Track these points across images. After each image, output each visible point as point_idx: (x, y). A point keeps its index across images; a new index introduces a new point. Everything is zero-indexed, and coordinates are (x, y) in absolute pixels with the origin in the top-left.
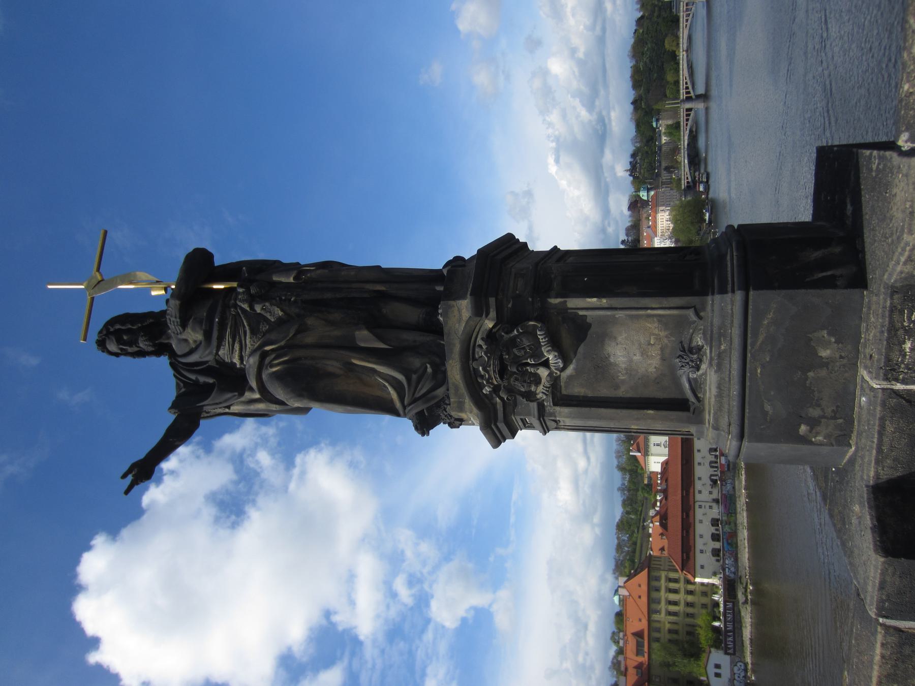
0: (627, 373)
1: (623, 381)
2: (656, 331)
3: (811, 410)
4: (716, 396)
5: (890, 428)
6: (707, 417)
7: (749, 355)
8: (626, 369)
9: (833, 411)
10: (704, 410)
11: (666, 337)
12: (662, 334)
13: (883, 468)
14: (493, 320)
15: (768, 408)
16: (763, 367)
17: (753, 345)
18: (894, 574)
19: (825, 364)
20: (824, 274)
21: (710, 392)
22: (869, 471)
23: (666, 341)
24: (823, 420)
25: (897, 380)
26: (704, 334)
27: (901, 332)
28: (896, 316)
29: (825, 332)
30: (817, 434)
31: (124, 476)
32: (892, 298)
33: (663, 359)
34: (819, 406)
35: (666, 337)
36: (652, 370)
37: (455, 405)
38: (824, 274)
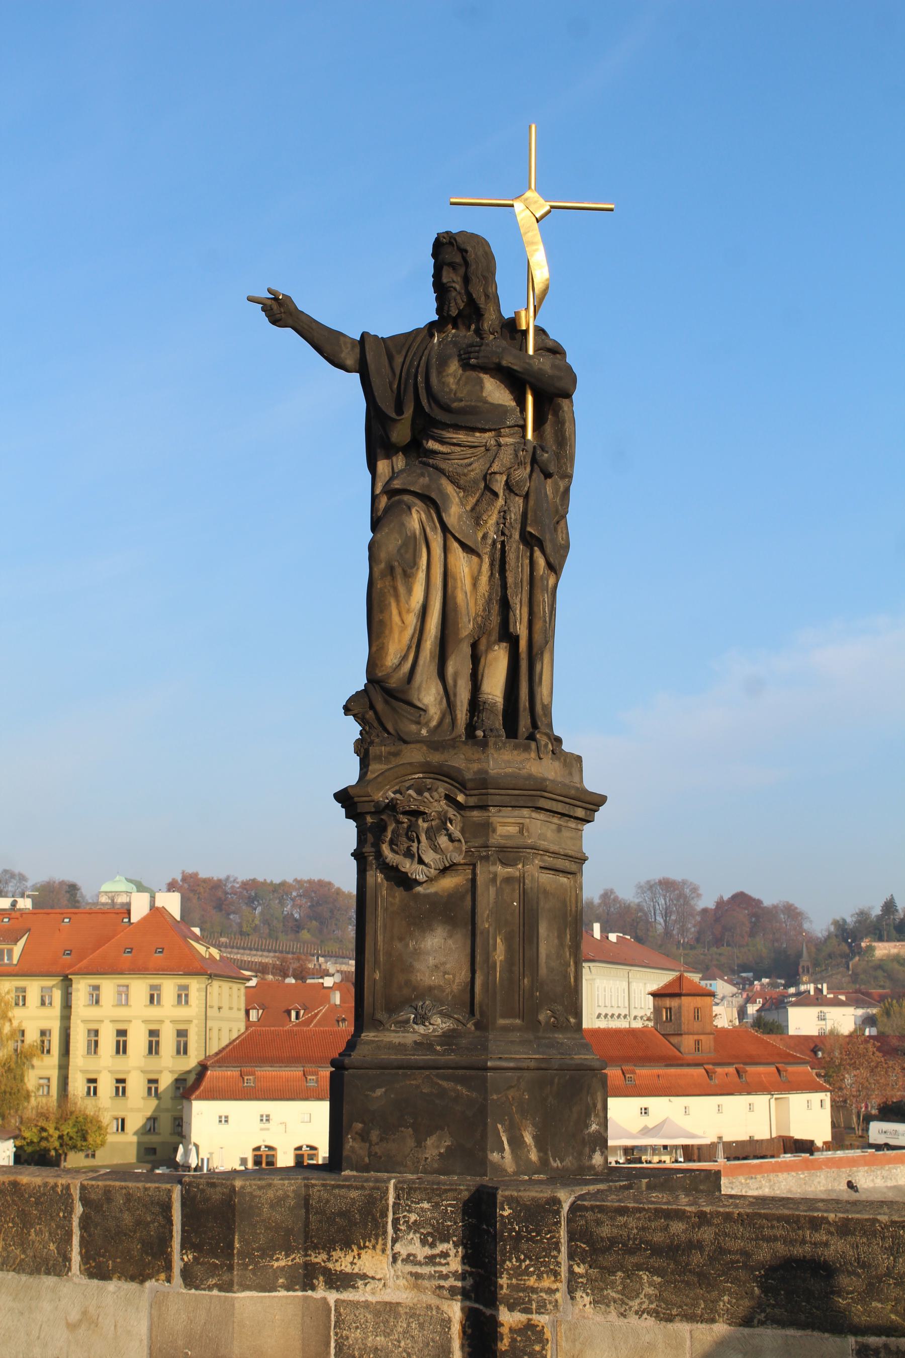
0: (416, 950)
1: (407, 945)
2: (457, 981)
3: (377, 1132)
4: (390, 1042)
5: (354, 1194)
6: (372, 1034)
7: (427, 1072)
8: (420, 948)
9: (376, 1153)
10: (378, 1031)
11: (452, 991)
12: (455, 987)
13: (319, 1191)
14: (466, 802)
15: (379, 1092)
16: (418, 1086)
17: (437, 1076)
18: (223, 1194)
19: (420, 1143)
20: (505, 1143)
21: (393, 1037)
22: (316, 1179)
23: (448, 990)
24: (368, 1145)
25: (398, 1197)
26: (454, 1030)
27: (437, 1199)
28: (450, 1194)
29: (448, 1143)
30: (354, 1139)
31: (270, 291)
32: (466, 1190)
33: (430, 989)
34: (381, 1140)
35: (452, 991)
36: (419, 976)
37: (378, 752)
38: (505, 1143)
